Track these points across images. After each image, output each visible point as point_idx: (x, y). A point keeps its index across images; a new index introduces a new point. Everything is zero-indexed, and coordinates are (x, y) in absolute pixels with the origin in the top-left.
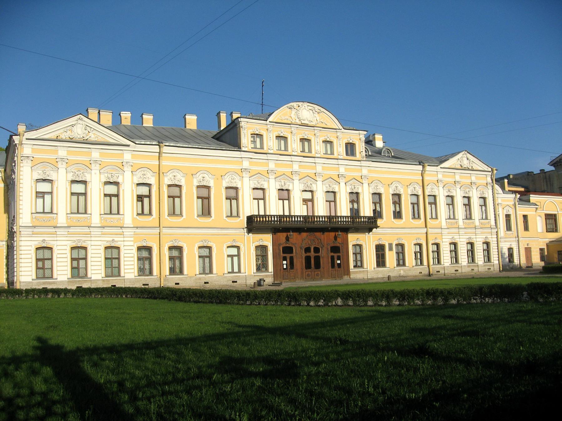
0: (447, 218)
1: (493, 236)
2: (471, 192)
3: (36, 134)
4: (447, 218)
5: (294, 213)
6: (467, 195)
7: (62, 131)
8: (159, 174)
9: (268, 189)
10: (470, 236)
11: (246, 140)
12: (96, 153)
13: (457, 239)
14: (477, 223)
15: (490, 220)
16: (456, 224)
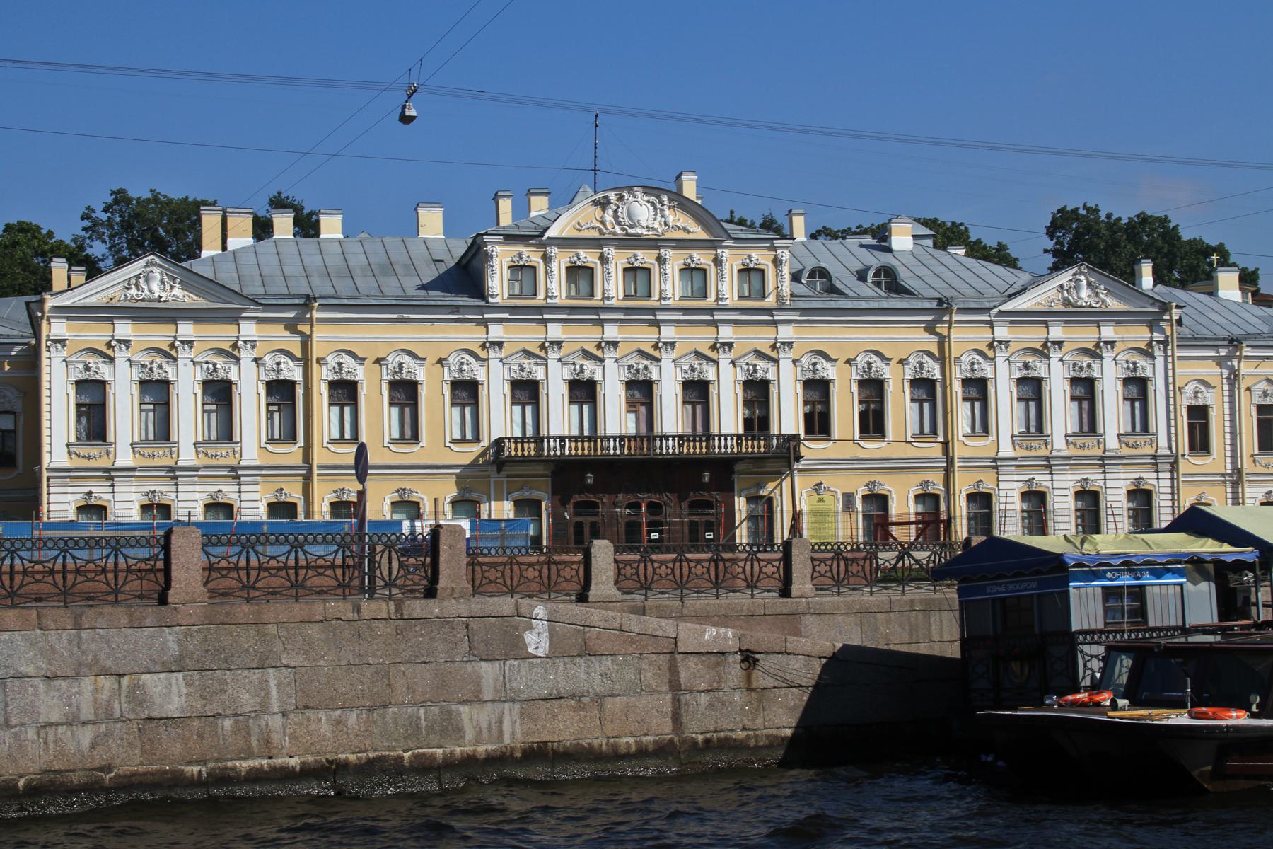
0: (1016, 432)
1: (1161, 475)
2: (1096, 367)
3: (73, 297)
4: (1016, 432)
5: (605, 430)
6: (1084, 375)
7: (120, 287)
8: (305, 360)
9: (486, 383)
10: (1085, 476)
11: (498, 284)
12: (186, 329)
13: (1044, 484)
14: (1112, 443)
15: (1156, 434)
16: (1043, 447)
